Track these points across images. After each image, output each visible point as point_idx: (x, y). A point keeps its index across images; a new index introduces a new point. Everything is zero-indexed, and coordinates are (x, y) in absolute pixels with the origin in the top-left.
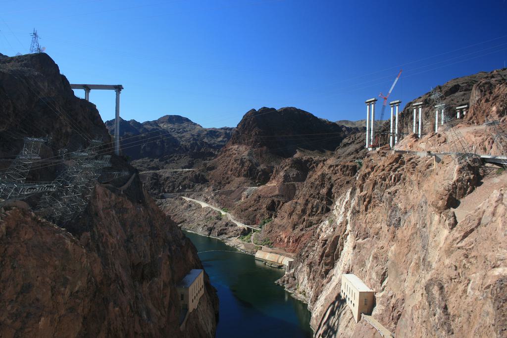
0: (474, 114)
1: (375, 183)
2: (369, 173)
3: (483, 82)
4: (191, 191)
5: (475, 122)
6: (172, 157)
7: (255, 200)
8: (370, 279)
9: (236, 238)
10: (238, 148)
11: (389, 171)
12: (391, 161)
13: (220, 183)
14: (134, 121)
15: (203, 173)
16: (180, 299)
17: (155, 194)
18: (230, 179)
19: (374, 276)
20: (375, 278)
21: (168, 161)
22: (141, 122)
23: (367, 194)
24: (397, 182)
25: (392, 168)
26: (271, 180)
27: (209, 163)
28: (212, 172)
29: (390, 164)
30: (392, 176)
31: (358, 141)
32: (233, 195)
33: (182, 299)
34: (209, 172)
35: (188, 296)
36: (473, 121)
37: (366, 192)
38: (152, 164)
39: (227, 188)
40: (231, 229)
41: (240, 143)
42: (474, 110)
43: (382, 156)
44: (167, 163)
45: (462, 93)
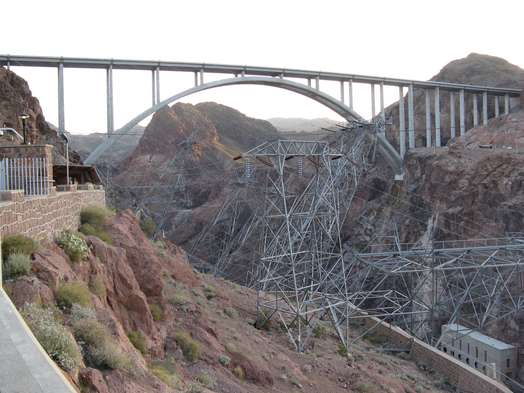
2: (455, 181)
7: (196, 228)
8: (503, 331)
10: (151, 158)
19: (513, 324)
20: (517, 328)
23: (462, 210)
25: (503, 173)
26: (209, 199)
37: (459, 208)
41: (152, 151)
43: (460, 157)
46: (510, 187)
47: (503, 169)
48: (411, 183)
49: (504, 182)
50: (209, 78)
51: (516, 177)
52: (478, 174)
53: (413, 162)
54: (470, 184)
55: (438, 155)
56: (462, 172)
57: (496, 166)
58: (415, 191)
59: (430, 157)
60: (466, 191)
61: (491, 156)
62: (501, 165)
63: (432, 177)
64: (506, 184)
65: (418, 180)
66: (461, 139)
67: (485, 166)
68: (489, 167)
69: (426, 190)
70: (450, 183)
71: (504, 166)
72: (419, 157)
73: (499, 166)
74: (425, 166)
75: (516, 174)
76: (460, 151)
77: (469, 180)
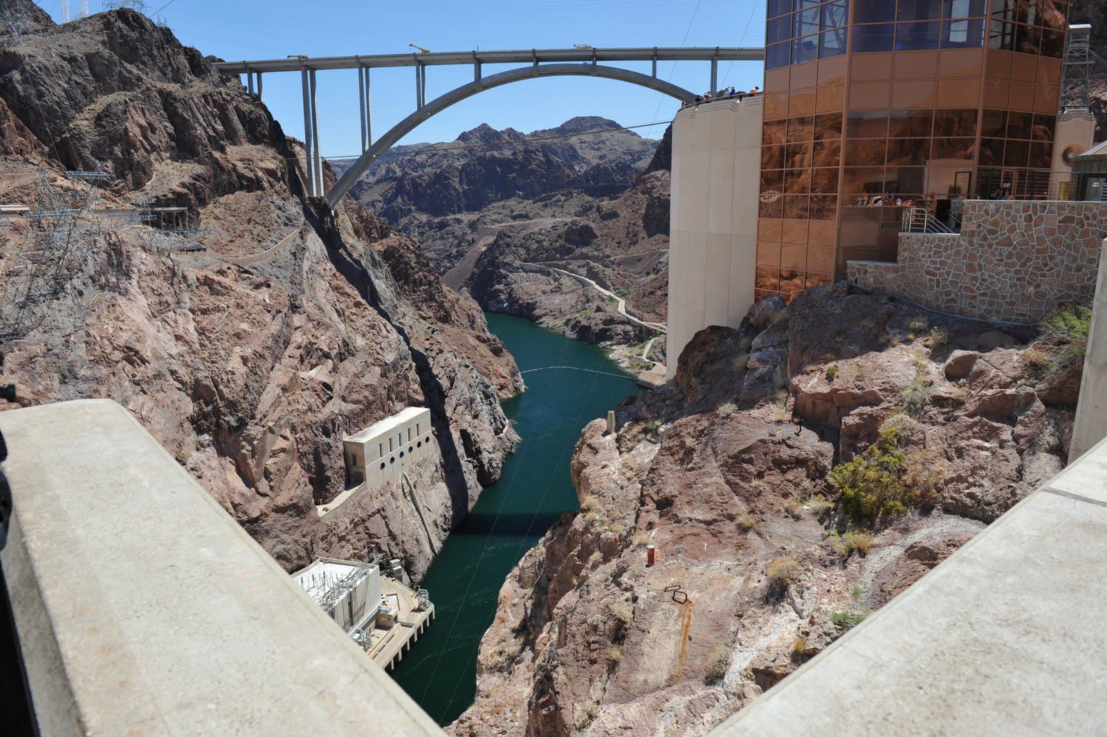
4: (570, 259)
6: (554, 196)
9: (624, 346)
13: (619, 243)
14: (511, 132)
15: (592, 225)
16: (351, 462)
17: (506, 264)
18: (641, 235)
21: (548, 202)
22: (527, 132)
27: (606, 204)
28: (609, 223)
32: (640, 266)
33: (355, 464)
34: (606, 223)
35: (363, 460)
38: (518, 210)
39: (634, 251)
40: (620, 328)
44: (546, 206)
50: (488, 70)
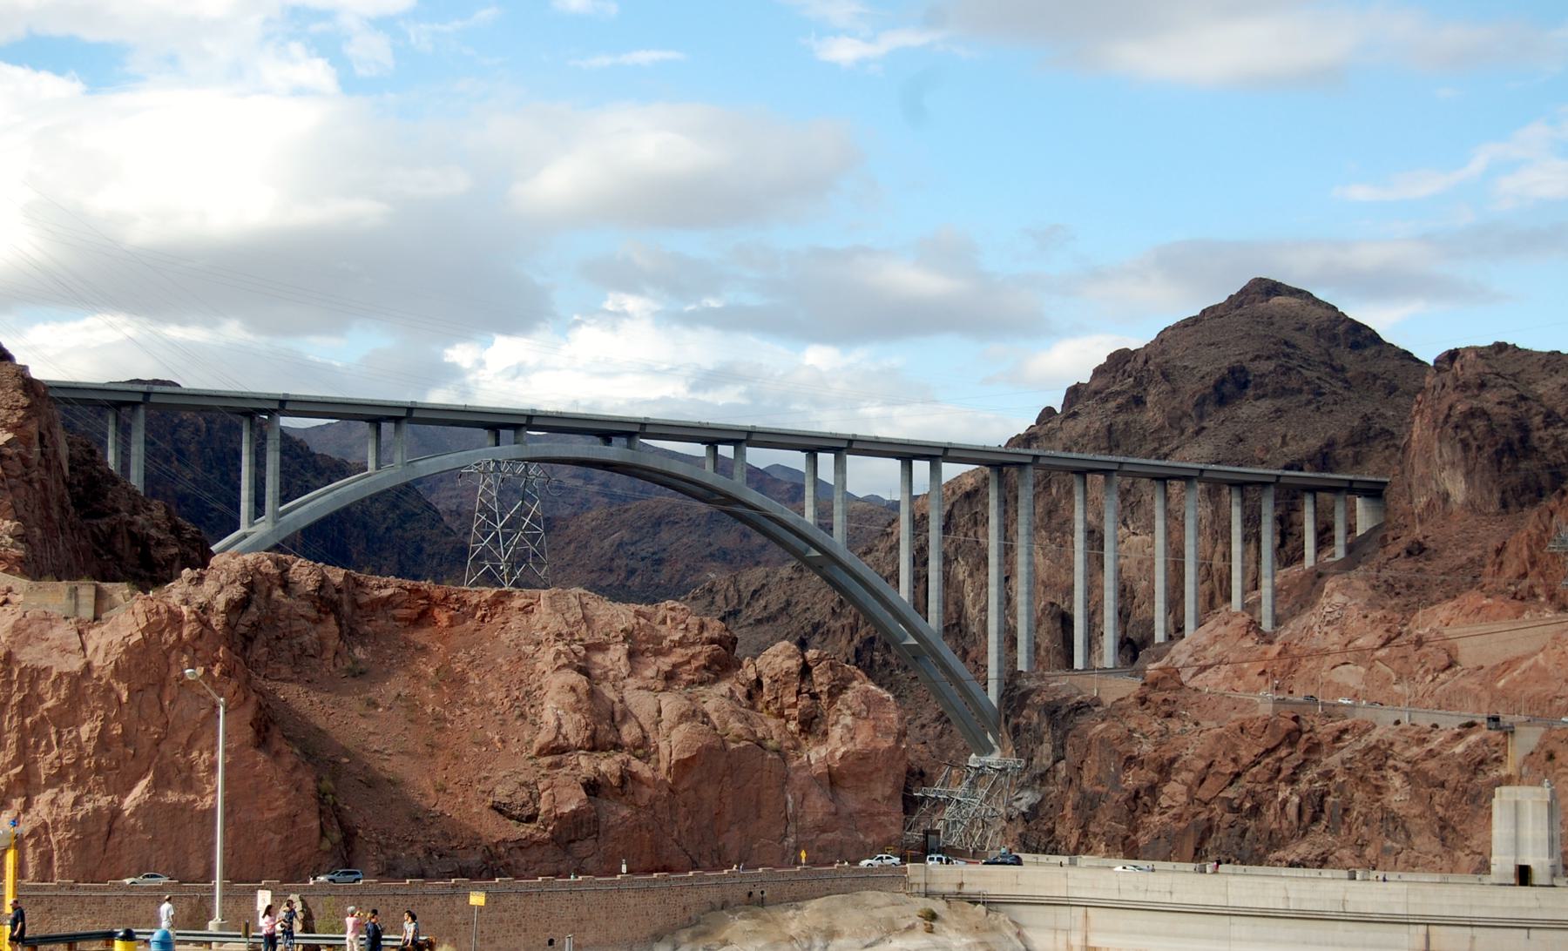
0: (1533, 564)
1: (1208, 830)
2: (1153, 789)
3: (1460, 407)
5: (1538, 591)
11: (1270, 780)
12: (1266, 741)
24: (1315, 819)
25: (1279, 770)
29: (1268, 752)
30: (1285, 802)
31: (757, 609)
36: (1531, 587)
42: (1529, 547)
43: (1169, 715)
45: (1265, 405)
46: (1292, 810)
47: (1281, 759)
48: (1023, 787)
49: (1281, 796)
51: (1310, 782)
52: (1212, 771)
53: (1029, 718)
54: (1192, 799)
55: (1108, 700)
56: (1172, 761)
57: (1262, 750)
58: (1034, 809)
59: (1081, 708)
60: (1178, 818)
61: (1251, 720)
62: (1274, 749)
63: (1085, 773)
64: (1285, 802)
65: (1043, 777)
66: (1180, 652)
67: (1234, 747)
68: (1243, 753)
69: (1068, 811)
70: (1136, 796)
71: (1283, 752)
72: (1047, 704)
73: (1268, 752)
74: (1066, 734)
75: (1312, 773)
76: (1170, 696)
77: (1190, 789)
